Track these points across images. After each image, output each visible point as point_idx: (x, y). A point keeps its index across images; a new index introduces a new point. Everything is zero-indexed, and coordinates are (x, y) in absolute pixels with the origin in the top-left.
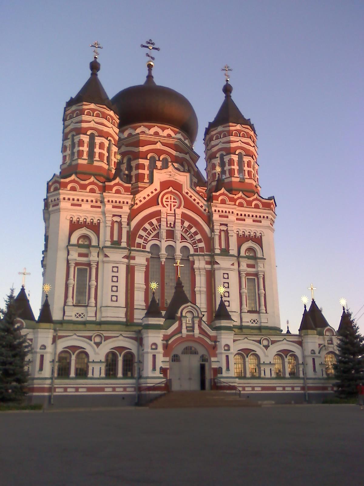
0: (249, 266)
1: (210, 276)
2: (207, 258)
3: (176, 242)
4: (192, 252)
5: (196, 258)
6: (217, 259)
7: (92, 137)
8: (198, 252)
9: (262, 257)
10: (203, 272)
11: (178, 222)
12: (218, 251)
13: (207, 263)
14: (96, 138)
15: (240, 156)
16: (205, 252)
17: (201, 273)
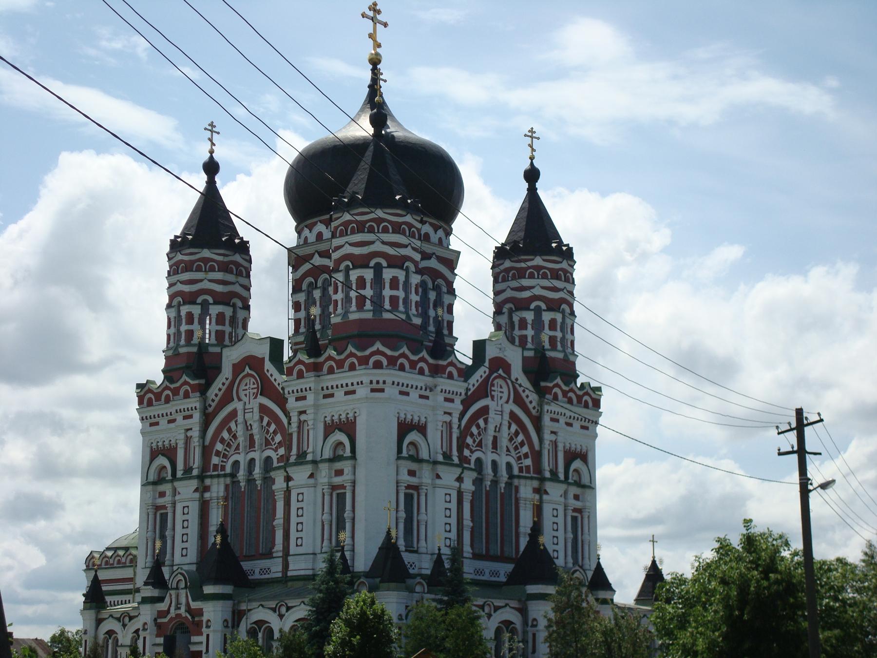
0: (576, 497)
1: (538, 510)
2: (536, 484)
3: (499, 455)
4: (516, 471)
5: (523, 481)
6: (549, 486)
7: (378, 269)
8: (523, 472)
9: (589, 484)
10: (530, 507)
11: (506, 423)
12: (547, 475)
13: (537, 491)
14: (384, 270)
15: (538, 311)
16: (532, 472)
17: (527, 505)
